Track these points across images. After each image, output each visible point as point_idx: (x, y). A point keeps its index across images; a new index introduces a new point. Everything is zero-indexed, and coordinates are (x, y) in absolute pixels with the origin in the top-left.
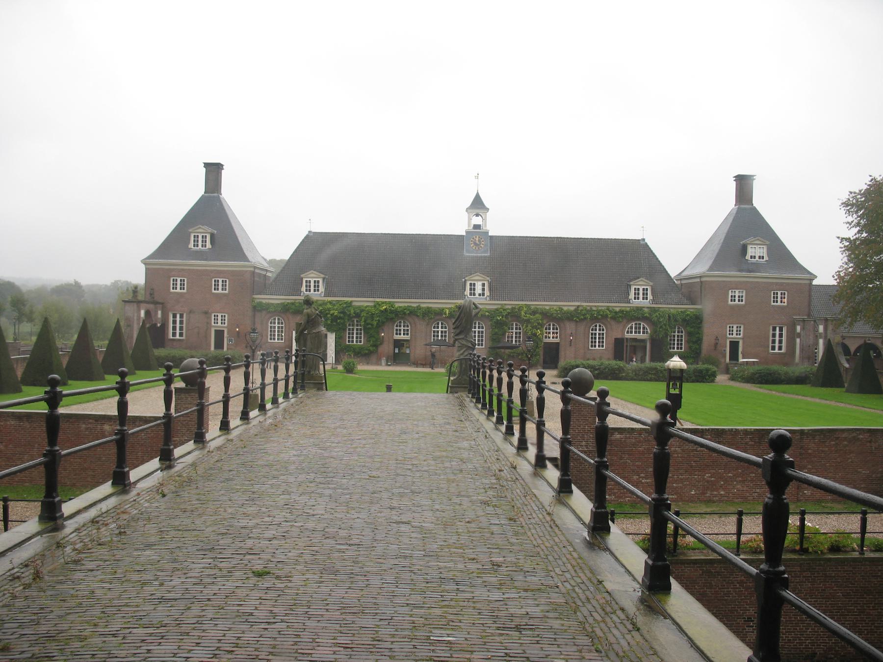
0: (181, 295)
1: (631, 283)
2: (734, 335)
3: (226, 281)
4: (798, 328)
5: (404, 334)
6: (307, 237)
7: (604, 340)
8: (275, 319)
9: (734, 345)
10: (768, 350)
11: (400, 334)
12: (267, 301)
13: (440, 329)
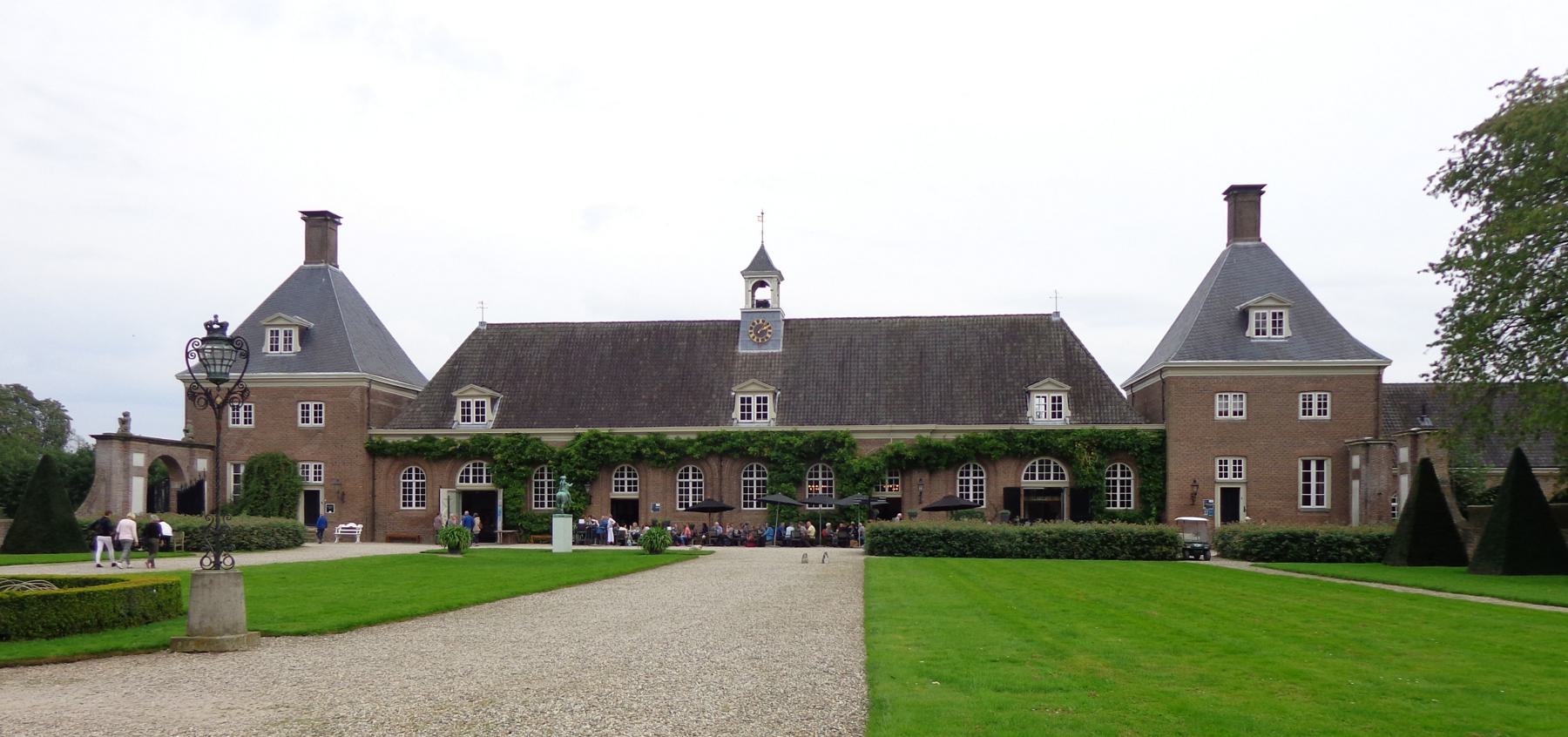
0: (246, 432)
1: (1030, 388)
2: (1230, 478)
3: (321, 406)
4: (1356, 461)
5: (629, 489)
6: (477, 332)
7: (984, 492)
8: (410, 470)
9: (1230, 496)
10: (1297, 505)
11: (623, 490)
12: (396, 439)
13: (690, 480)
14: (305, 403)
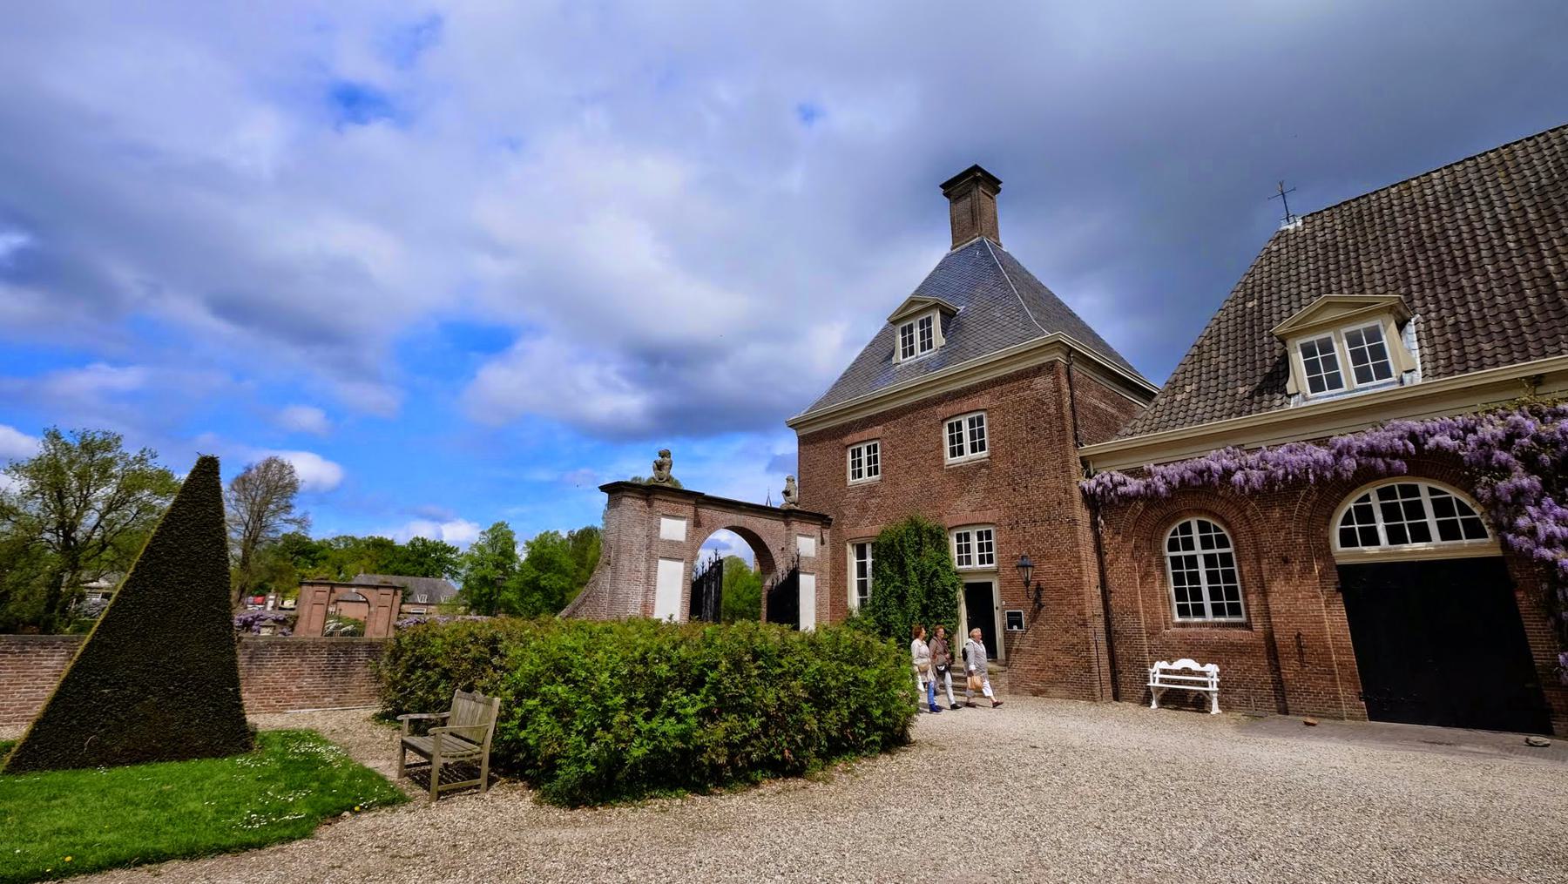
0: (871, 490)
8: (1186, 528)
14: (954, 421)
